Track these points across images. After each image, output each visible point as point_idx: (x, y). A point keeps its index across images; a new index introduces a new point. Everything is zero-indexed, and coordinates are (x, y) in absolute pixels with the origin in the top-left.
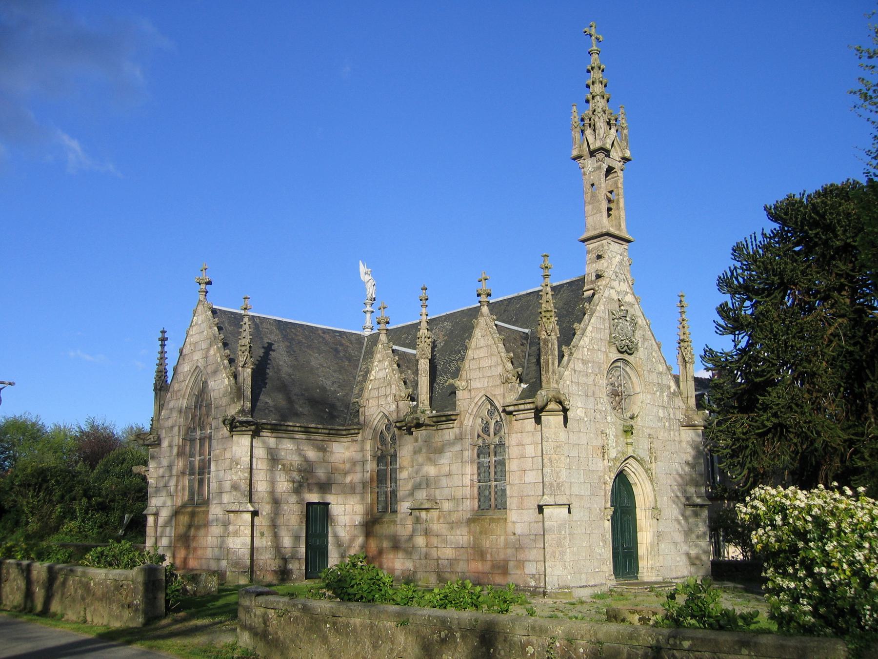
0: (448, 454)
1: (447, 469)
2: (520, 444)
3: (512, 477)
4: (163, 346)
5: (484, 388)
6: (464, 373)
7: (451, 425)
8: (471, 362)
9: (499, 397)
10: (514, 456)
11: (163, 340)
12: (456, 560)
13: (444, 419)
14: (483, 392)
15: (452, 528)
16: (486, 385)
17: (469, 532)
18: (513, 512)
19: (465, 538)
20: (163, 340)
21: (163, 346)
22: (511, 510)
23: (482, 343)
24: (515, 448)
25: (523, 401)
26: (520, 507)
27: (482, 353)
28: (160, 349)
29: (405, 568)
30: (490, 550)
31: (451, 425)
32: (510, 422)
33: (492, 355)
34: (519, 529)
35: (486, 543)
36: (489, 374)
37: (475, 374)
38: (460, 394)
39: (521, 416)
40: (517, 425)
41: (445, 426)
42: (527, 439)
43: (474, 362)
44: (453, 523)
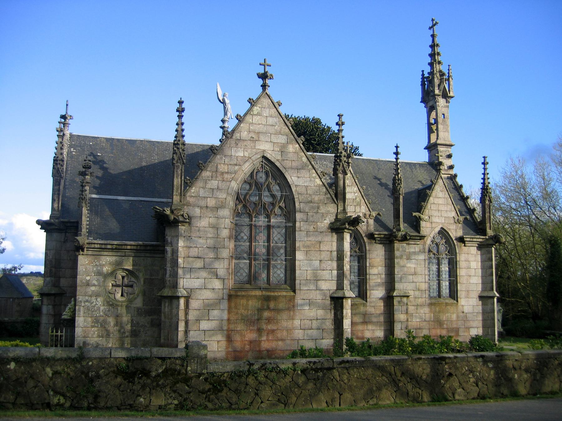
0: (413, 261)
1: (413, 270)
2: (467, 261)
3: (462, 279)
4: (180, 117)
5: (442, 223)
6: (427, 211)
7: (418, 243)
8: (432, 206)
9: (452, 231)
10: (463, 267)
11: (181, 111)
12: (420, 329)
13: (419, 238)
14: (441, 226)
15: (417, 309)
16: (443, 221)
17: (431, 311)
18: (462, 300)
19: (427, 315)
20: (181, 111)
21: (180, 117)
22: (460, 298)
23: (441, 195)
24: (464, 262)
25: (469, 237)
26: (467, 297)
27: (441, 201)
28: (177, 120)
29: (375, 336)
30: (446, 322)
31: (418, 243)
32: (461, 247)
33: (448, 204)
34: (466, 309)
35: (444, 317)
36: (446, 216)
37: (435, 213)
38: (423, 224)
39: (469, 245)
40: (465, 249)
41: (413, 243)
42: (471, 258)
43: (435, 206)
44: (417, 305)
